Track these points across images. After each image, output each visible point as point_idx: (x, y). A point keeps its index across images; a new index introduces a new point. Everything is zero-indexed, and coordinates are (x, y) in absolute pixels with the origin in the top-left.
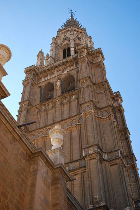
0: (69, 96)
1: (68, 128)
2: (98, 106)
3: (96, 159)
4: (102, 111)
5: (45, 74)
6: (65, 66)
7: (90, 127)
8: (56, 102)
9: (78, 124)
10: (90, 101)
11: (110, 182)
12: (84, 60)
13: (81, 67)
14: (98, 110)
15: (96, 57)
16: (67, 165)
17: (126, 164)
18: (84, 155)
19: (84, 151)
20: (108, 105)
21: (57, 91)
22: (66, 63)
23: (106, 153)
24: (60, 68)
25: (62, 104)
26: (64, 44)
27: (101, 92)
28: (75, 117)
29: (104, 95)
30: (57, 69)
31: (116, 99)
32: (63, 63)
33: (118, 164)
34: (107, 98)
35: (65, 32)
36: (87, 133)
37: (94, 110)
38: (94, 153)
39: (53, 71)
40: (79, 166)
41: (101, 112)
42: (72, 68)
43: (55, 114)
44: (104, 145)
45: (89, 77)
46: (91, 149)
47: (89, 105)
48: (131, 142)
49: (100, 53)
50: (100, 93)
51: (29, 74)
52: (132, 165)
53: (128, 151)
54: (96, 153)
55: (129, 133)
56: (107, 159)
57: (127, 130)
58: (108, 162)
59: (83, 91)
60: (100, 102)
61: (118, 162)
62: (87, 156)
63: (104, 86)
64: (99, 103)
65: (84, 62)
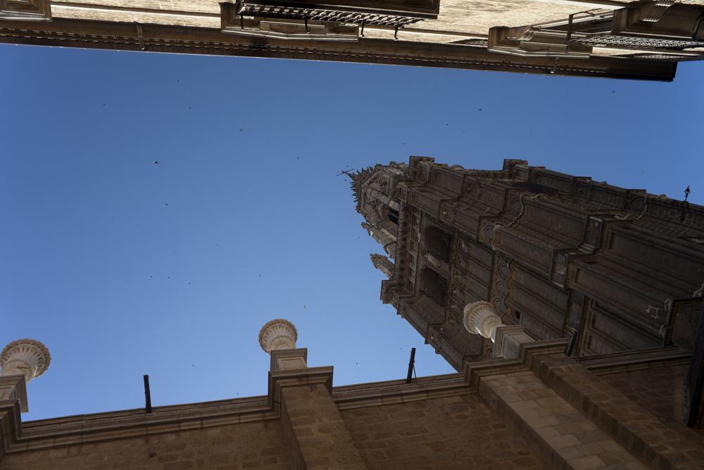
2: (496, 212)
9: (508, 265)
16: (567, 326)
18: (562, 286)
33: (614, 232)
37: (497, 224)
41: (511, 212)
44: (568, 238)
46: (558, 266)
48: (605, 183)
50: (480, 196)
52: (648, 203)
54: (568, 263)
56: (594, 247)
57: (579, 180)
58: (601, 250)
61: (610, 231)
62: (566, 282)
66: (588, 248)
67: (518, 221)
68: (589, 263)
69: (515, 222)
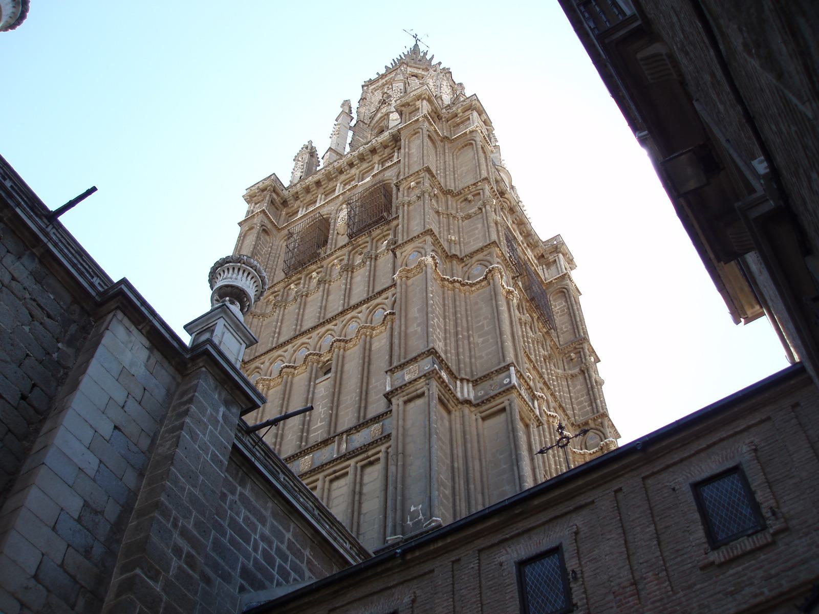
0: (372, 242)
1: (359, 331)
2: (455, 251)
3: (426, 394)
4: (469, 265)
5: (309, 197)
6: (367, 165)
7: (416, 309)
8: (333, 268)
9: (388, 312)
10: (422, 234)
11: (477, 467)
12: (418, 128)
13: (407, 150)
14: (455, 262)
15: (462, 122)
16: (344, 436)
17: (583, 447)
19: (391, 378)
20: (488, 242)
21: (340, 236)
22: (369, 153)
23: (468, 381)
24: (354, 171)
25: (349, 269)
26: (379, 115)
27: (470, 212)
28: (384, 295)
29: (478, 219)
30: (343, 177)
31: (551, 258)
32: (362, 154)
33: (508, 408)
34: (486, 225)
35: (384, 85)
36: (406, 327)
37: (433, 257)
38: (420, 378)
39: (331, 185)
40: (382, 434)
41: (465, 269)
42: (387, 165)
43: (324, 302)
44: (467, 360)
45: (428, 170)
47: (420, 245)
48: (600, 383)
49: (475, 109)
50: (469, 217)
51: (259, 202)
53: (588, 408)
54: (425, 375)
55: (596, 354)
57: (586, 346)
58: (473, 409)
59: (406, 211)
60: (466, 241)
62: (396, 389)
63: (479, 194)
64: (462, 245)
65: (417, 135)
66: (466, 391)
67: (457, 285)
68: (440, 400)
69: (454, 281)
